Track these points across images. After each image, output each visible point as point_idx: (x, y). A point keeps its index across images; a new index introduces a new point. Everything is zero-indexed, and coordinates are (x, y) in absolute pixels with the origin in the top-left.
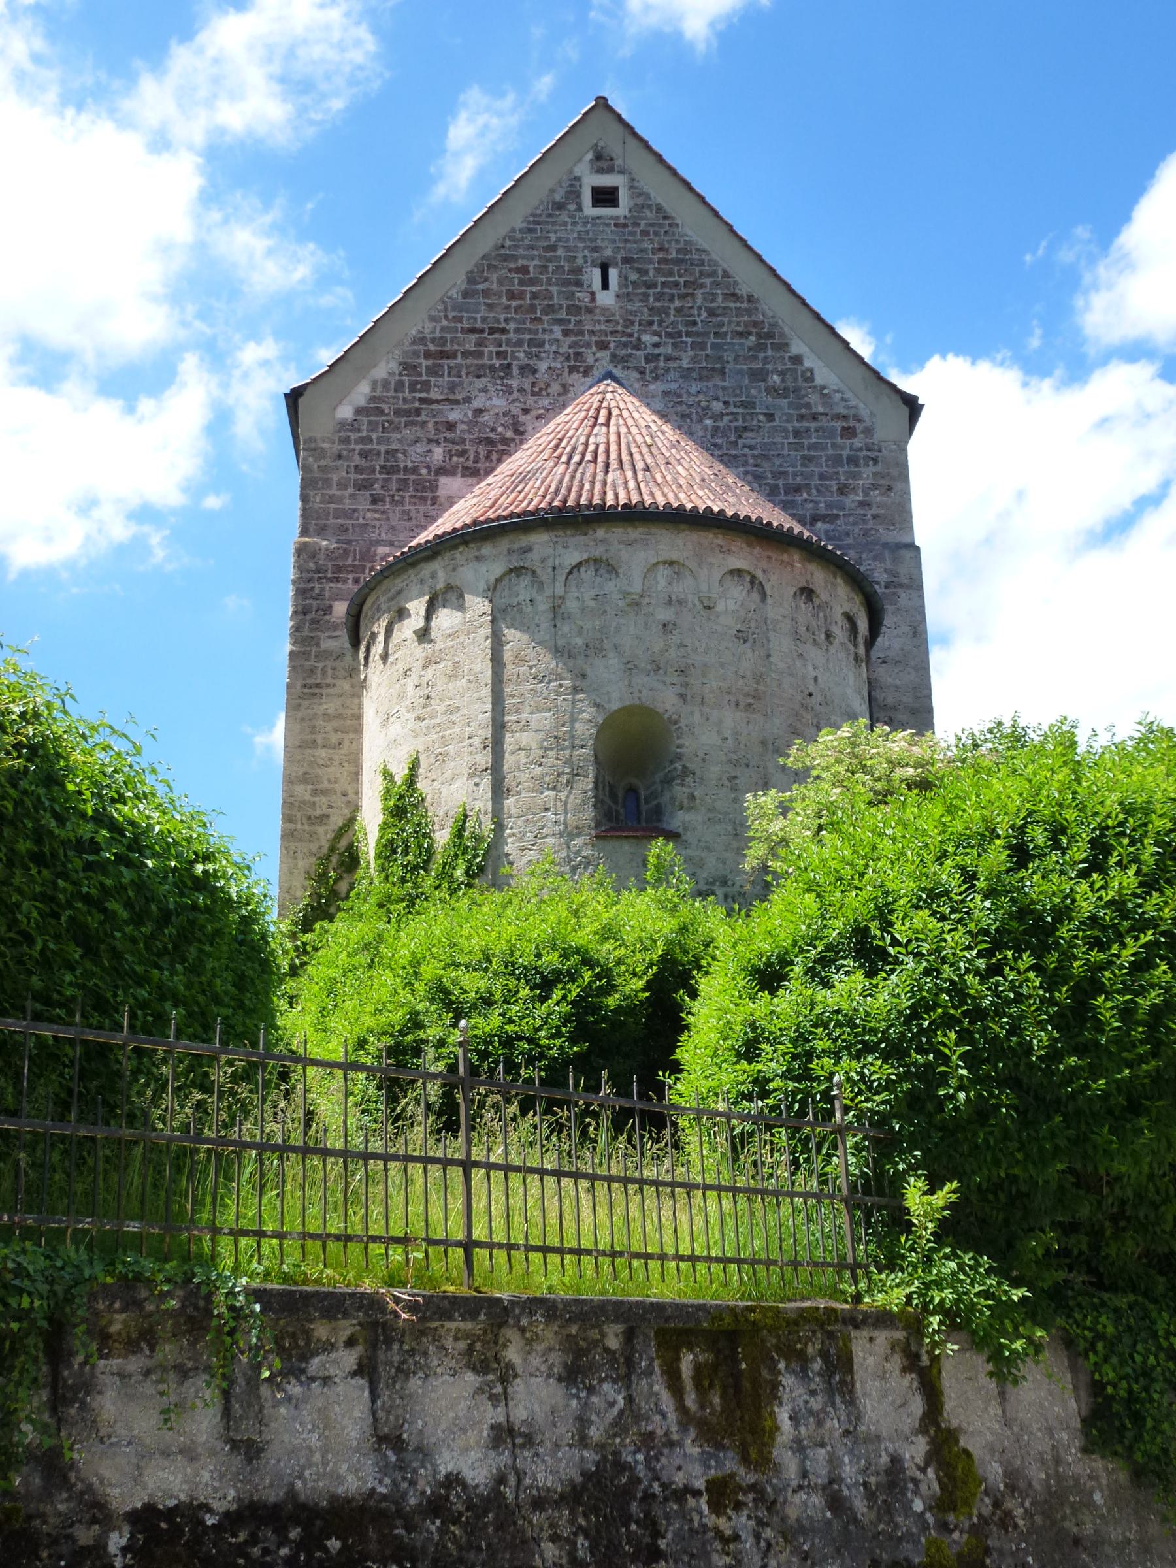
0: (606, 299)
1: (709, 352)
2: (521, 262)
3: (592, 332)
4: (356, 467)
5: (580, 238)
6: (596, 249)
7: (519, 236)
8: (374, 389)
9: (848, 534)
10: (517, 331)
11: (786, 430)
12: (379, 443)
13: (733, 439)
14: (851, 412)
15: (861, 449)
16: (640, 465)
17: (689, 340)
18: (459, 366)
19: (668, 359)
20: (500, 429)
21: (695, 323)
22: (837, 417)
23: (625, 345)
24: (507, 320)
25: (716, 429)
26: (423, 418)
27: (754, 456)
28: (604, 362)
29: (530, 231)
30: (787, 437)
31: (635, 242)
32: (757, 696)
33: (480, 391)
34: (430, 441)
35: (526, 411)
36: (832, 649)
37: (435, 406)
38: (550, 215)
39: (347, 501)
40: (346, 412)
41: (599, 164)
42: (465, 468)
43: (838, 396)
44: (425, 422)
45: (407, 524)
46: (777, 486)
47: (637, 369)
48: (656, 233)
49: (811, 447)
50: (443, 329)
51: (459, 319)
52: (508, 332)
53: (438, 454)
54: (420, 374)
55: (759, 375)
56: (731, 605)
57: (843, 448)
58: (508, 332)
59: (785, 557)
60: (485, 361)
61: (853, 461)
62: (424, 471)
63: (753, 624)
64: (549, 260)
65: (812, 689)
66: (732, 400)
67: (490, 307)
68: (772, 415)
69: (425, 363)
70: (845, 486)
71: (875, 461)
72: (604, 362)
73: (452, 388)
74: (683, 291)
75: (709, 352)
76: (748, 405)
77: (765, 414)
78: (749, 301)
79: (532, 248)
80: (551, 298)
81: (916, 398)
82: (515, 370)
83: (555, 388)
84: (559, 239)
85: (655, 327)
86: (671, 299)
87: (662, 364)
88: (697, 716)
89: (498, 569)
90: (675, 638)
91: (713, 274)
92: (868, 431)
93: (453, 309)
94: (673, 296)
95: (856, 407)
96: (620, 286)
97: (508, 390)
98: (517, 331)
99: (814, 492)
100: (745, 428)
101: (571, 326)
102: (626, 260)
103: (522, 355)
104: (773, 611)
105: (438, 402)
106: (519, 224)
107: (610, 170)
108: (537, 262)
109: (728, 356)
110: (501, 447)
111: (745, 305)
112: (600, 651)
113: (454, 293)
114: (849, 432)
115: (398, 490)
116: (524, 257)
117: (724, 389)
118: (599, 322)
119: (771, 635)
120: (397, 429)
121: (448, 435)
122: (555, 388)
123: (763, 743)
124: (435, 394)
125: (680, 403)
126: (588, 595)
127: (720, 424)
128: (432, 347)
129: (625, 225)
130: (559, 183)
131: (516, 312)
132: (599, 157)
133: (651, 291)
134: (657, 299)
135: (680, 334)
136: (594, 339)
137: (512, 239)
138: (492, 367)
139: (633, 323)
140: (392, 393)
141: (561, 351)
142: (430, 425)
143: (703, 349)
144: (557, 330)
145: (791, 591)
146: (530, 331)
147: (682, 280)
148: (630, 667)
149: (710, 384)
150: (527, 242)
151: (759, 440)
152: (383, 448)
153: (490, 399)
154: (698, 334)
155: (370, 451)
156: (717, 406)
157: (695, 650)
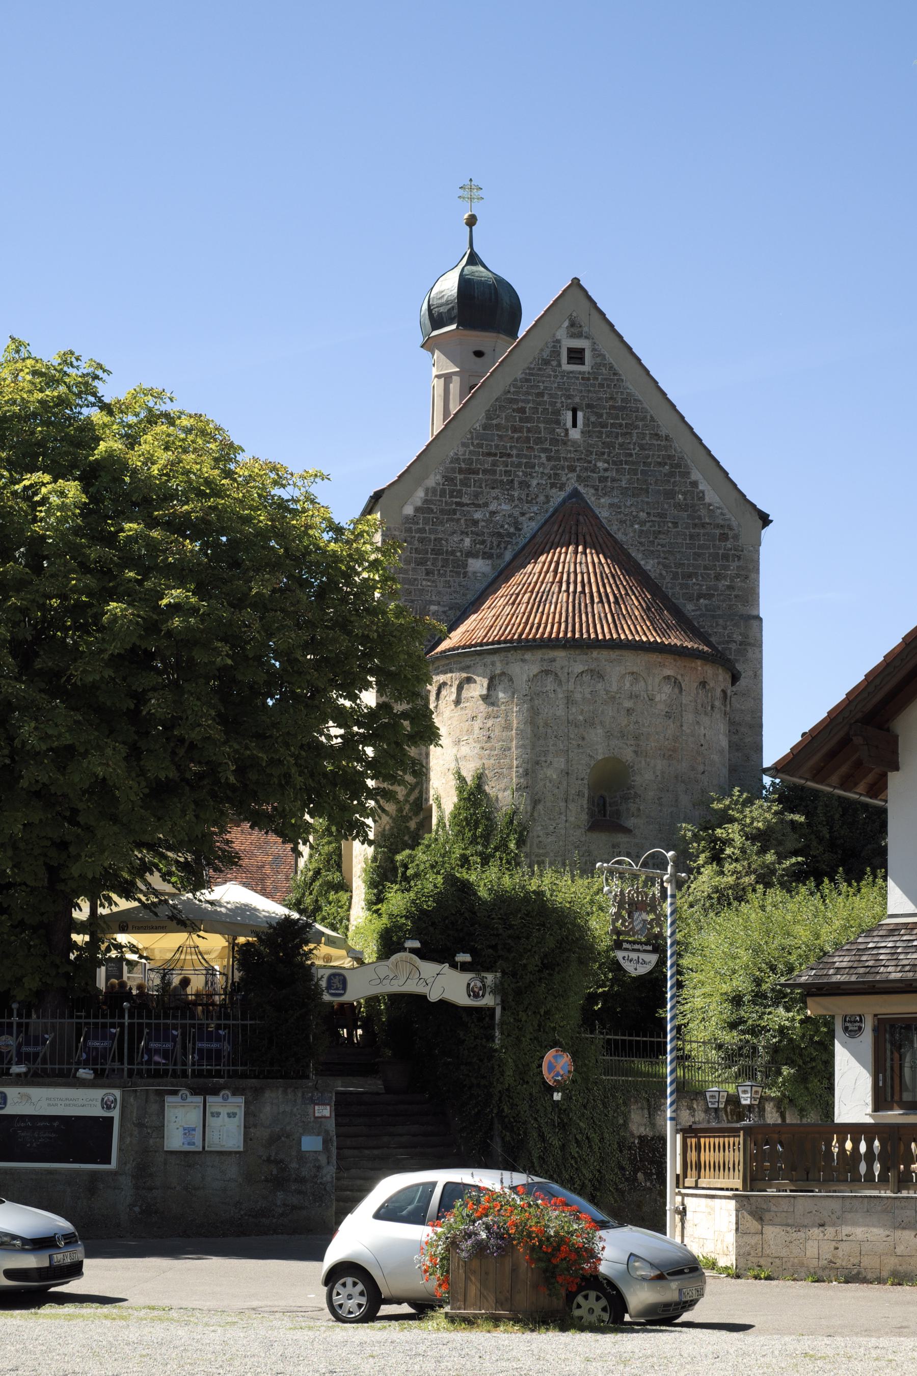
0: (575, 434)
1: (639, 476)
2: (521, 405)
3: (565, 459)
4: (416, 549)
5: (559, 388)
6: (569, 397)
7: (519, 384)
8: (426, 494)
9: (719, 608)
10: (518, 456)
11: (685, 534)
12: (430, 533)
13: (651, 539)
14: (727, 523)
15: (731, 549)
16: (612, 599)
17: (627, 467)
18: (480, 479)
19: (613, 480)
20: (506, 526)
21: (631, 455)
22: (718, 526)
23: (586, 469)
24: (511, 447)
25: (641, 531)
26: (458, 516)
27: (663, 552)
28: (573, 481)
29: (527, 380)
30: (685, 539)
31: (595, 392)
32: (674, 750)
33: (494, 498)
34: (462, 533)
35: (523, 514)
36: (714, 714)
37: (465, 508)
38: (540, 369)
39: (410, 573)
40: (409, 510)
41: (572, 330)
42: (484, 553)
43: (719, 511)
44: (459, 519)
45: (449, 590)
46: (677, 572)
47: (593, 487)
48: (609, 386)
49: (700, 547)
50: (470, 452)
51: (480, 446)
52: (512, 456)
53: (467, 542)
54: (456, 485)
55: (670, 494)
56: (664, 697)
57: (719, 549)
58: (512, 456)
59: (693, 665)
60: (497, 477)
61: (725, 557)
62: (458, 554)
63: (674, 707)
64: (539, 404)
65: (702, 742)
66: (652, 511)
67: (501, 437)
68: (677, 523)
69: (459, 477)
70: (720, 574)
71: (739, 558)
72: (573, 481)
73: (476, 495)
74: (625, 430)
75: (639, 476)
76: (662, 515)
77: (672, 523)
78: (666, 440)
79: (528, 393)
80: (540, 433)
81: (768, 515)
82: (516, 485)
83: (541, 498)
84: (545, 388)
85: (605, 457)
86: (617, 437)
87: (609, 484)
88: (643, 762)
89: (535, 669)
90: (633, 718)
91: (643, 419)
92: (736, 537)
93: (477, 439)
94: (618, 433)
95: (729, 520)
96: (585, 425)
97: (512, 499)
98: (518, 456)
99: (700, 578)
100: (660, 532)
101: (552, 454)
102: (589, 406)
103: (521, 474)
104: (685, 699)
105: (467, 505)
106: (519, 375)
107: (579, 335)
108: (531, 405)
109: (651, 480)
110: (506, 539)
111: (663, 443)
112: (592, 725)
113: (477, 426)
114: (724, 537)
115: (442, 566)
116: (523, 401)
117: (648, 503)
118: (570, 451)
119: (684, 713)
120: (442, 523)
121: (473, 529)
122: (541, 498)
123: (676, 777)
124: (466, 500)
125: (620, 513)
126: (587, 690)
127: (645, 529)
128: (463, 465)
129: (588, 379)
130: (546, 343)
131: (517, 442)
132: (572, 324)
133: (604, 430)
134: (607, 436)
135: (621, 462)
136: (566, 464)
137: (515, 386)
138: (502, 481)
139: (591, 453)
140: (438, 498)
141: (546, 471)
142: (462, 521)
143: (636, 474)
144: (543, 455)
145: (696, 685)
146: (526, 456)
147: (624, 422)
148: (609, 735)
149: (639, 499)
150: (524, 389)
151: (668, 540)
152: (433, 537)
153: (500, 505)
154: (633, 463)
155: (425, 538)
156: (643, 515)
157: (643, 725)
